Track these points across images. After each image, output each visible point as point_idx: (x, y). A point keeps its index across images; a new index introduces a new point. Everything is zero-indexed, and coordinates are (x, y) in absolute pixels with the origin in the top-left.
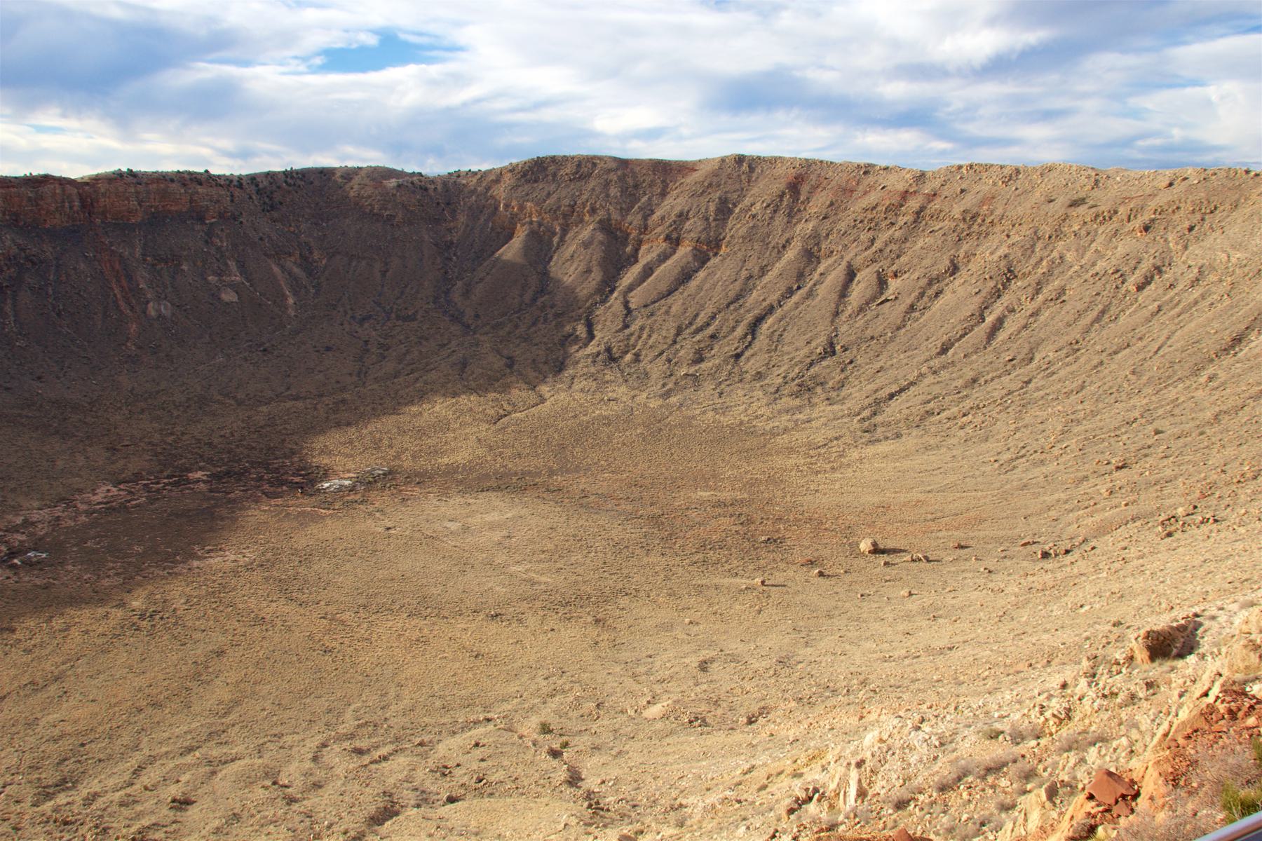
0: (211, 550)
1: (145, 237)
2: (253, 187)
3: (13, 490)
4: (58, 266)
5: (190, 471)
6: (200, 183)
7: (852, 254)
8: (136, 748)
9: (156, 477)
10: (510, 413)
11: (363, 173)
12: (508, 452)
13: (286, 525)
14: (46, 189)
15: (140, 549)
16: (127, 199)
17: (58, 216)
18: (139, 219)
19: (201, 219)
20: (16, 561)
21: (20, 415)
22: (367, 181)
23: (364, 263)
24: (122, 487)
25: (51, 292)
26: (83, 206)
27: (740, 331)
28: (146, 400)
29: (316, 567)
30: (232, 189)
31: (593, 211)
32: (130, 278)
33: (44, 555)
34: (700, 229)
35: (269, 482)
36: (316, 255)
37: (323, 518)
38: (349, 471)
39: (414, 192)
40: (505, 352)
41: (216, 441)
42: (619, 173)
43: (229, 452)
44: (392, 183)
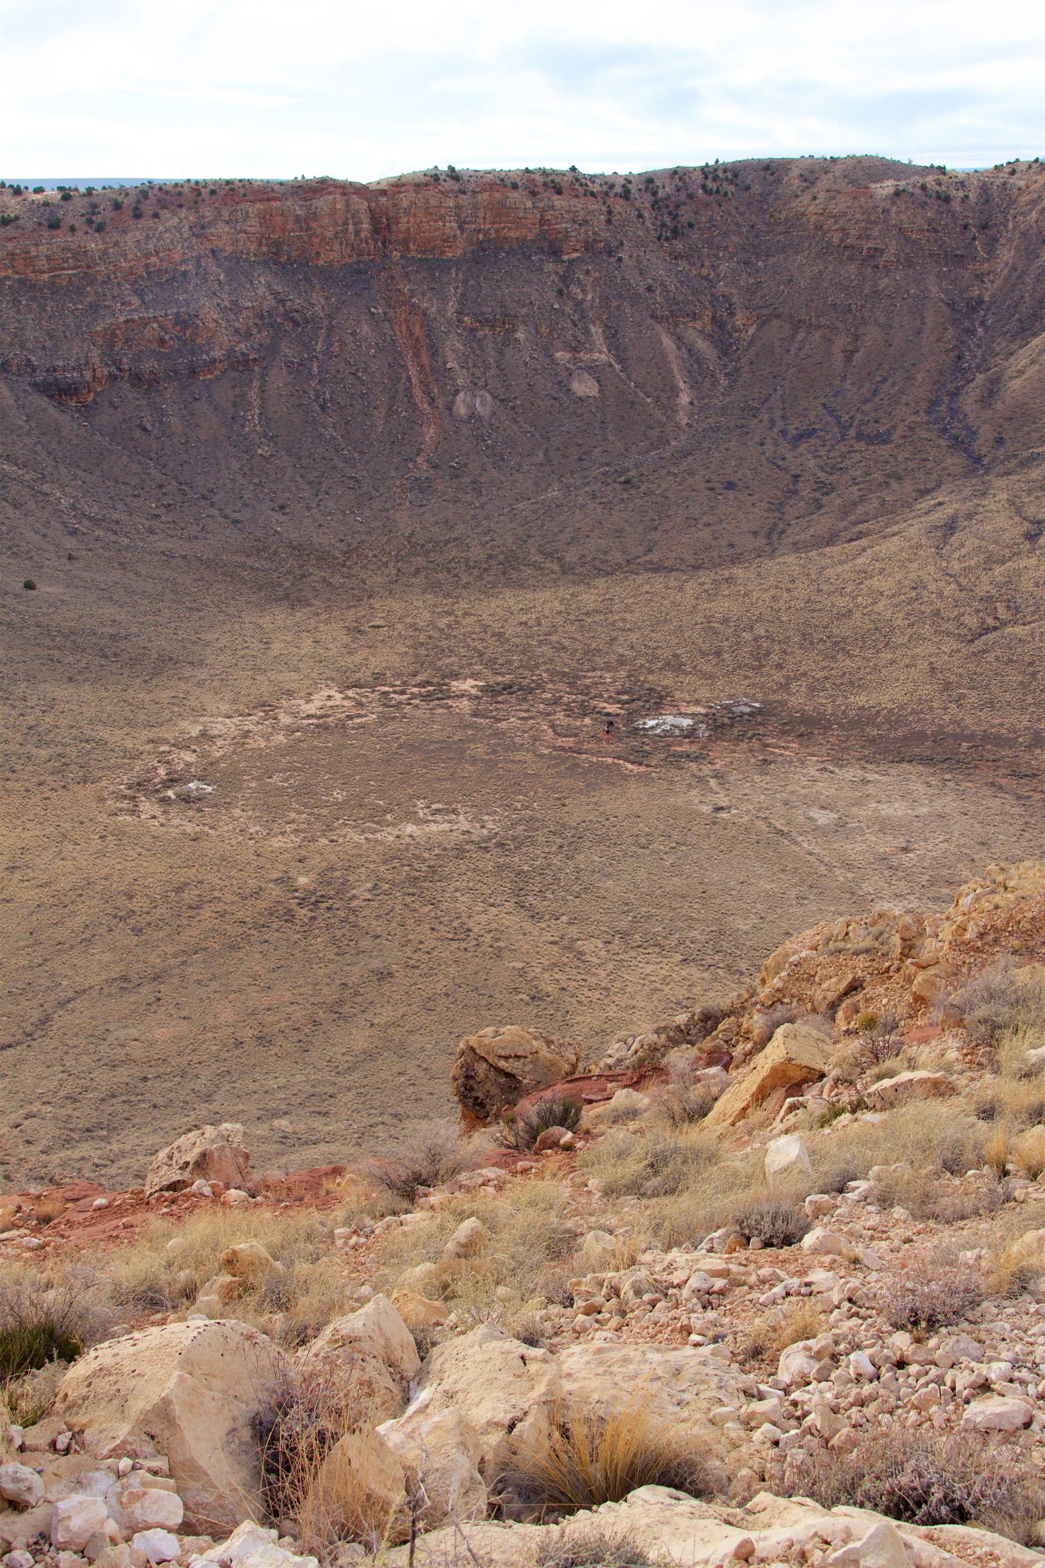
0: (438, 811)
1: (466, 281)
2: (648, 197)
3: (200, 684)
4: (330, 329)
5: (456, 676)
6: (559, 192)
8: (209, 1098)
9: (404, 683)
10: (1004, 624)
11: (837, 170)
12: (973, 698)
13: (564, 782)
14: (322, 203)
15: (339, 796)
16: (442, 218)
17: (336, 246)
18: (459, 252)
19: (555, 253)
20: (170, 793)
21: (243, 566)
22: (842, 185)
23: (817, 335)
24: (350, 693)
25: (316, 370)
26: (376, 230)
28: (427, 553)
29: (580, 857)
30: (610, 201)
32: (434, 351)
33: (209, 789)
35: (569, 710)
36: (739, 320)
37: (626, 778)
38: (697, 702)
39: (923, 205)
40: (1031, 511)
41: (510, 631)
43: (524, 652)
44: (885, 188)
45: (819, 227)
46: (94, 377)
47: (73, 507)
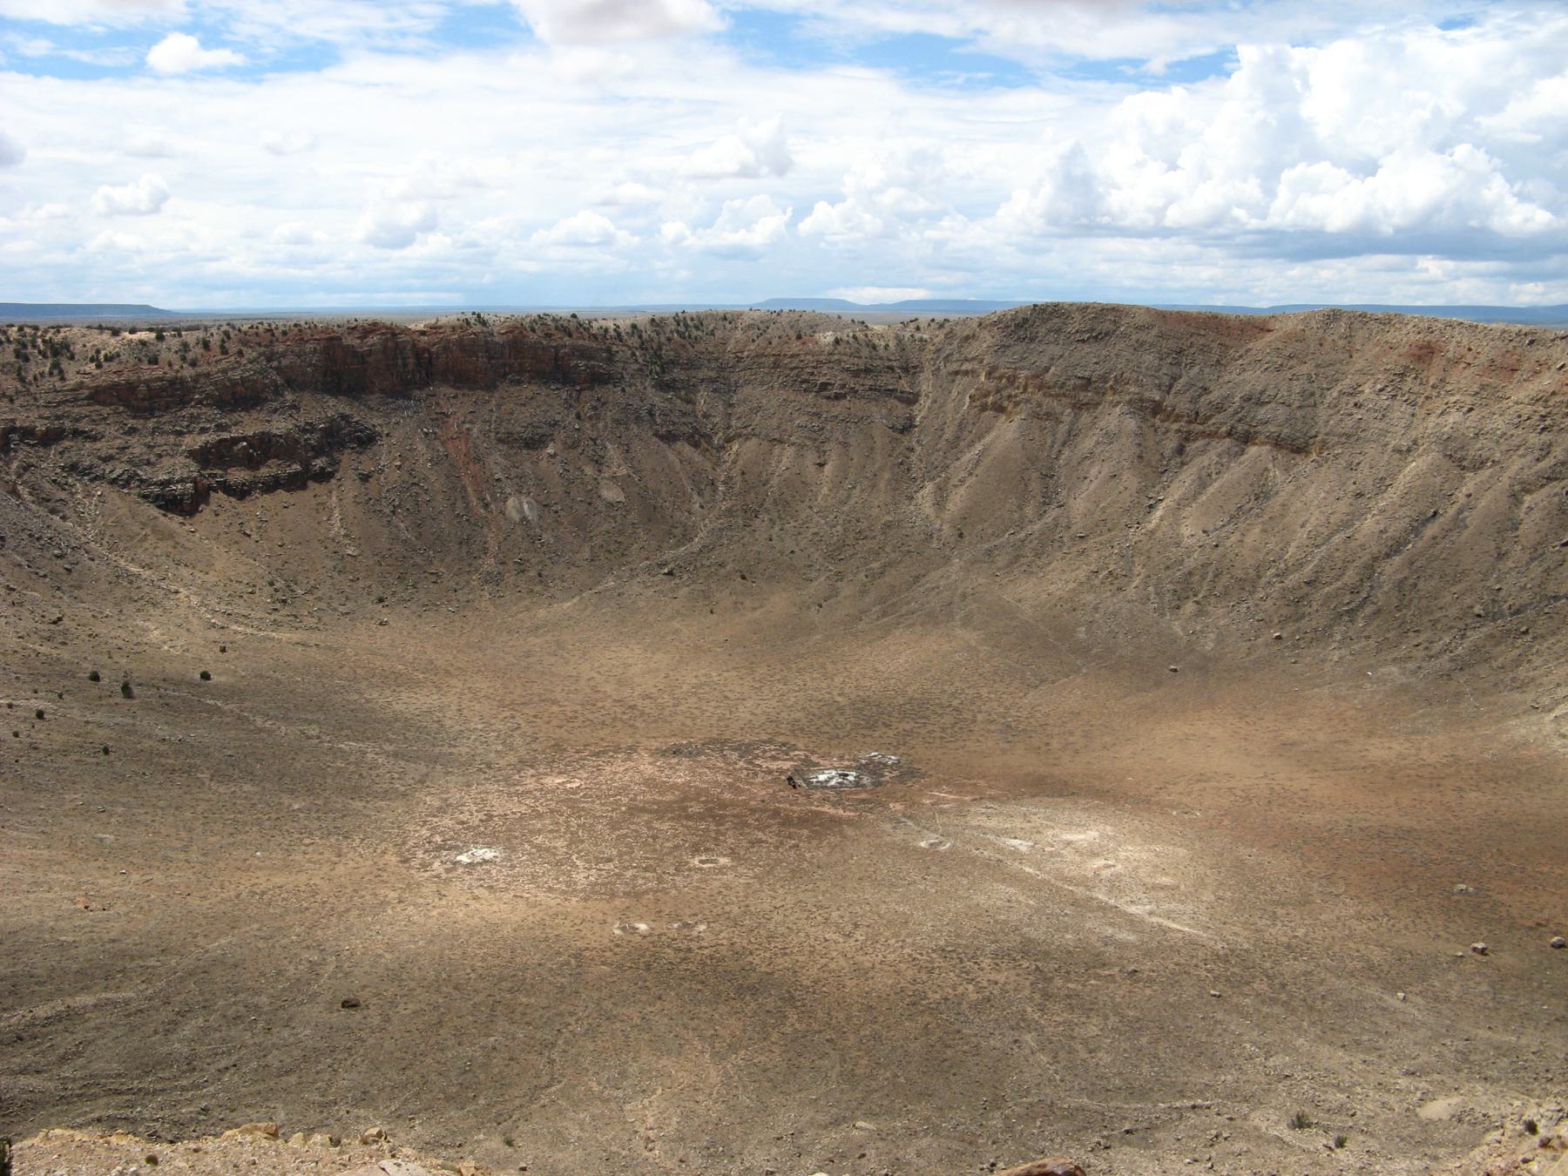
2: (635, 341)
7: (1515, 468)
14: (374, 339)
26: (418, 364)
27: (1350, 576)
34: (1282, 419)
42: (1154, 332)
44: (827, 338)
45: (776, 365)
46: (195, 488)
47: (202, 604)
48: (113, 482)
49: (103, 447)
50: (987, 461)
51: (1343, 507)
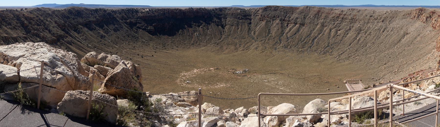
31: (278, 17)
48: (143, 29)
49: (142, 25)
50: (261, 27)
51: (309, 32)
